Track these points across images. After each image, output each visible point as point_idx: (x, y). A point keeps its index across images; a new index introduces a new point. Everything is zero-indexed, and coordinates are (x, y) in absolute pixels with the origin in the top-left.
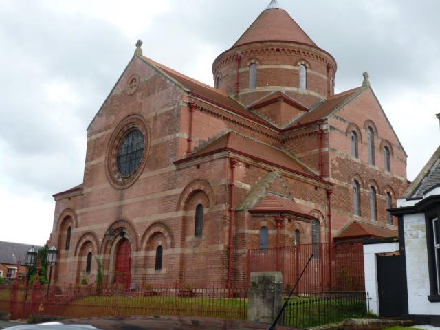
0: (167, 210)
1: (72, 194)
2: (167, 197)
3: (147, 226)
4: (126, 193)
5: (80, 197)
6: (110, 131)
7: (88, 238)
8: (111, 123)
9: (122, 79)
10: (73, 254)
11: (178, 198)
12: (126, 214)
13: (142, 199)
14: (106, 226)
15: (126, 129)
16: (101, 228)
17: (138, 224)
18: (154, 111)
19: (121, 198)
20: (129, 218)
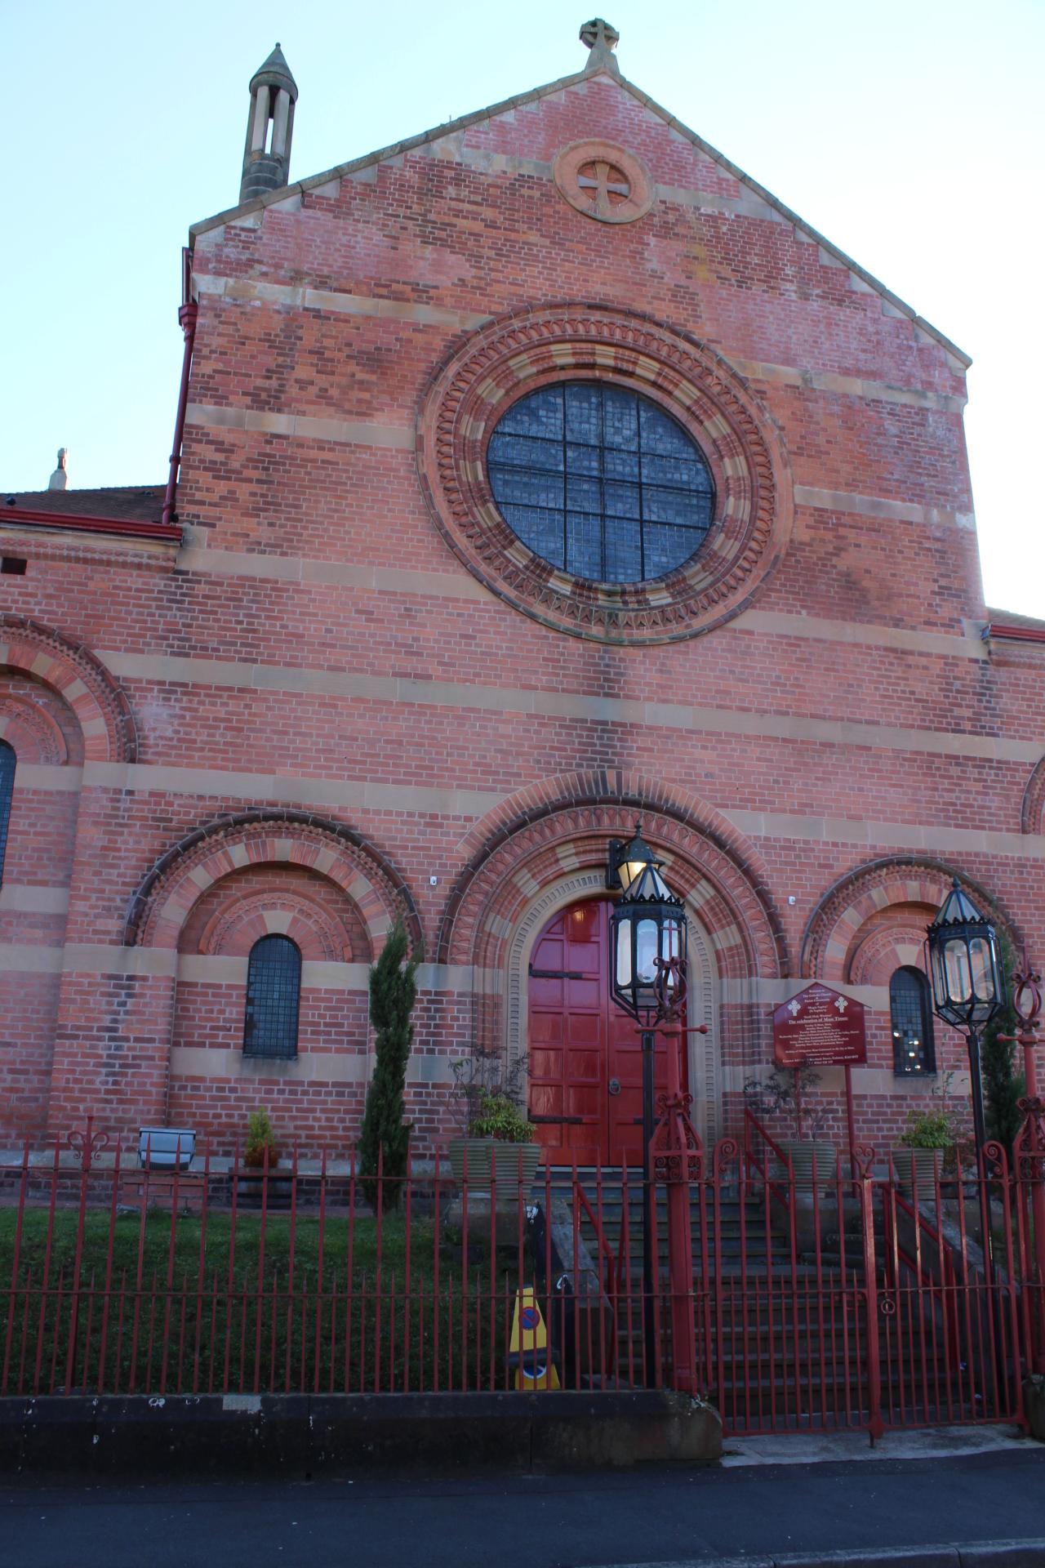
0: (963, 817)
1: (67, 540)
2: (953, 759)
3: (845, 864)
4: (640, 669)
5: (159, 582)
6: (454, 322)
7: (327, 857)
8: (445, 281)
9: (509, 117)
10: (115, 925)
11: (1023, 778)
12: (646, 772)
13: (783, 727)
14: (478, 807)
15: (563, 355)
16: (432, 815)
17: (767, 843)
18: (788, 361)
19: (605, 684)
20: (681, 796)
